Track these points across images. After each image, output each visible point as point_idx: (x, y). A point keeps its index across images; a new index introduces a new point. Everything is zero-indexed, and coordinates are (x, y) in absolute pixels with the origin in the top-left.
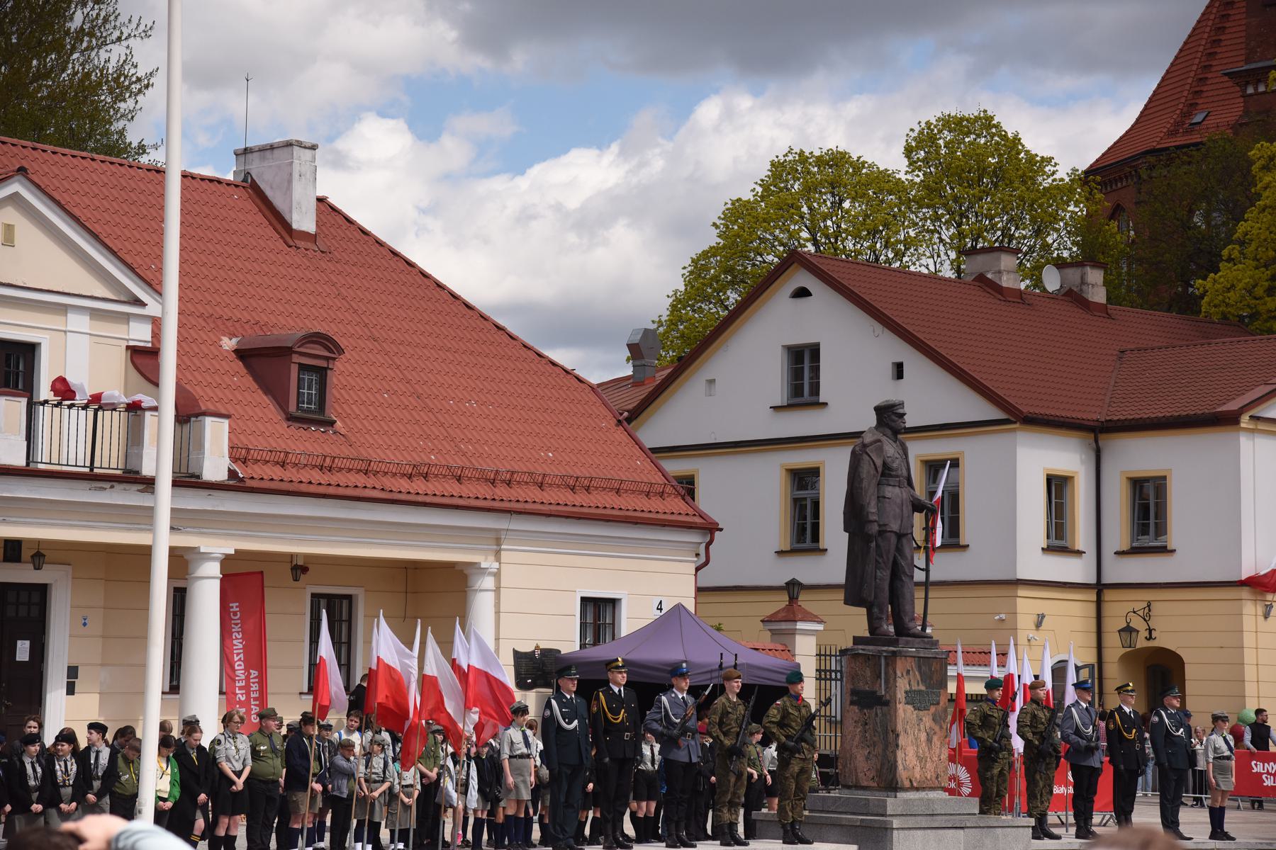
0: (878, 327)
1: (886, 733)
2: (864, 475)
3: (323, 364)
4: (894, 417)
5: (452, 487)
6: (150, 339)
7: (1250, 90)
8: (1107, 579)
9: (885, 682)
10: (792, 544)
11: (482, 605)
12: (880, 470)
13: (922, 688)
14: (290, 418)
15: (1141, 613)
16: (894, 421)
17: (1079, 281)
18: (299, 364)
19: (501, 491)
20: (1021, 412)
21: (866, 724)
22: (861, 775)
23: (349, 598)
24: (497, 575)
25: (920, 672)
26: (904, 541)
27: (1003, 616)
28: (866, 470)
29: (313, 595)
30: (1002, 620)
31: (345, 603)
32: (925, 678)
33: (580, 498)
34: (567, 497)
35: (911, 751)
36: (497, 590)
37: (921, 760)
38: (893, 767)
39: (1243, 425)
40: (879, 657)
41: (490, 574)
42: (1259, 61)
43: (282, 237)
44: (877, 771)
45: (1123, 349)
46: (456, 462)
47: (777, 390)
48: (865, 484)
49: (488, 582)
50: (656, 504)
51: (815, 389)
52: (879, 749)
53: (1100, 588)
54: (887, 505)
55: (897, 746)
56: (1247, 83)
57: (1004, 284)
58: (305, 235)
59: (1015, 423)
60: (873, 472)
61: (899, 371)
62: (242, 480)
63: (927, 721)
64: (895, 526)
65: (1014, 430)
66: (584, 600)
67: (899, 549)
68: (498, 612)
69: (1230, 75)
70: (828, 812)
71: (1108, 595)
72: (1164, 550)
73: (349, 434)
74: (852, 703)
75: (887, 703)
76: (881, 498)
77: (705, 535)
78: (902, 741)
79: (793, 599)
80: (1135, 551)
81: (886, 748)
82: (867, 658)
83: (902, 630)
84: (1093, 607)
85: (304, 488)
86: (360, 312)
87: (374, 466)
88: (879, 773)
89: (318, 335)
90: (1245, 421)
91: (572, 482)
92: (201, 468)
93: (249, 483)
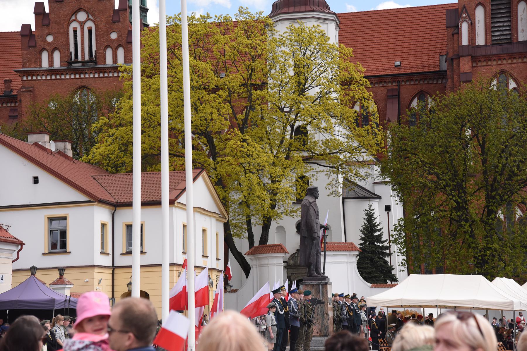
0: (25, 161)
1: (323, 314)
2: (312, 214)
7: (25, 78)
8: (115, 265)
9: (322, 294)
17: (63, 147)
20: (98, 198)
27: (88, 280)
30: (87, 282)
40: (319, 285)
42: (29, 68)
44: (319, 329)
45: (92, 175)
48: (313, 217)
53: (114, 268)
57: (47, 147)
59: (95, 202)
60: (314, 213)
61: (36, 180)
65: (93, 205)
69: (15, 71)
79: (33, 274)
81: (323, 320)
84: (110, 276)
90: (176, 202)
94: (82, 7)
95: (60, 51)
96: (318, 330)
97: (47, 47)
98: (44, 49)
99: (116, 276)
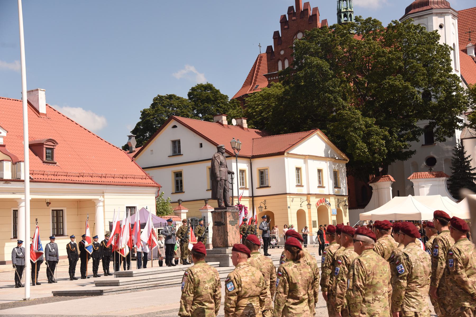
1: (224, 232)
3: (52, 147)
4: (222, 149)
5: (90, 179)
6: (3, 142)
7: (269, 79)
8: (254, 195)
10: (175, 191)
11: (100, 211)
12: (220, 163)
13: (233, 220)
14: (44, 162)
15: (263, 203)
16: (222, 150)
18: (46, 148)
19: (103, 179)
21: (219, 230)
22: (218, 244)
23: (62, 210)
24: (104, 202)
25: (232, 215)
26: (226, 182)
28: (216, 164)
29: (52, 210)
31: (61, 212)
32: (234, 217)
33: (124, 180)
34: (121, 180)
35: (231, 236)
36: (104, 206)
37: (234, 238)
38: (227, 241)
39: (285, 155)
41: (101, 202)
42: (271, 72)
43: (37, 115)
45: (253, 138)
46: (91, 172)
47: (169, 151)
48: (216, 167)
49: (101, 204)
50: (144, 181)
51: (180, 151)
52: (223, 237)
54: (222, 173)
55: (228, 235)
56: (269, 77)
58: (43, 114)
60: (218, 164)
61: (201, 145)
62: (32, 179)
63: (234, 227)
64: (224, 178)
66: (127, 207)
67: (225, 184)
68: (104, 212)
69: (264, 75)
70: (210, 254)
71: (255, 199)
72: (268, 187)
73: (61, 166)
74: (215, 225)
75: (224, 225)
76: (220, 171)
77: (158, 188)
78: (229, 234)
80: (261, 187)
82: (219, 213)
83: (227, 205)
85: (50, 181)
86: (60, 134)
87: (68, 174)
88: (223, 243)
89: (51, 139)
90: (286, 153)
91: (122, 176)
92: (21, 176)
93: (35, 180)
94: (300, 30)
95: (281, 61)
96: (222, 243)
97: (281, 58)
98: (279, 60)
99: (255, 202)
